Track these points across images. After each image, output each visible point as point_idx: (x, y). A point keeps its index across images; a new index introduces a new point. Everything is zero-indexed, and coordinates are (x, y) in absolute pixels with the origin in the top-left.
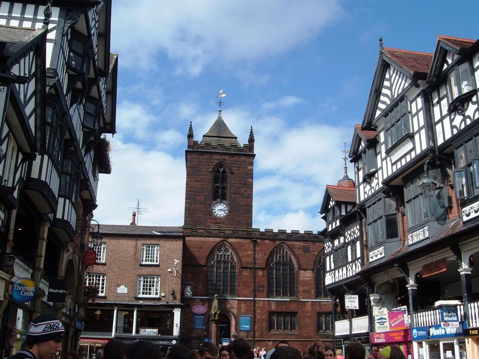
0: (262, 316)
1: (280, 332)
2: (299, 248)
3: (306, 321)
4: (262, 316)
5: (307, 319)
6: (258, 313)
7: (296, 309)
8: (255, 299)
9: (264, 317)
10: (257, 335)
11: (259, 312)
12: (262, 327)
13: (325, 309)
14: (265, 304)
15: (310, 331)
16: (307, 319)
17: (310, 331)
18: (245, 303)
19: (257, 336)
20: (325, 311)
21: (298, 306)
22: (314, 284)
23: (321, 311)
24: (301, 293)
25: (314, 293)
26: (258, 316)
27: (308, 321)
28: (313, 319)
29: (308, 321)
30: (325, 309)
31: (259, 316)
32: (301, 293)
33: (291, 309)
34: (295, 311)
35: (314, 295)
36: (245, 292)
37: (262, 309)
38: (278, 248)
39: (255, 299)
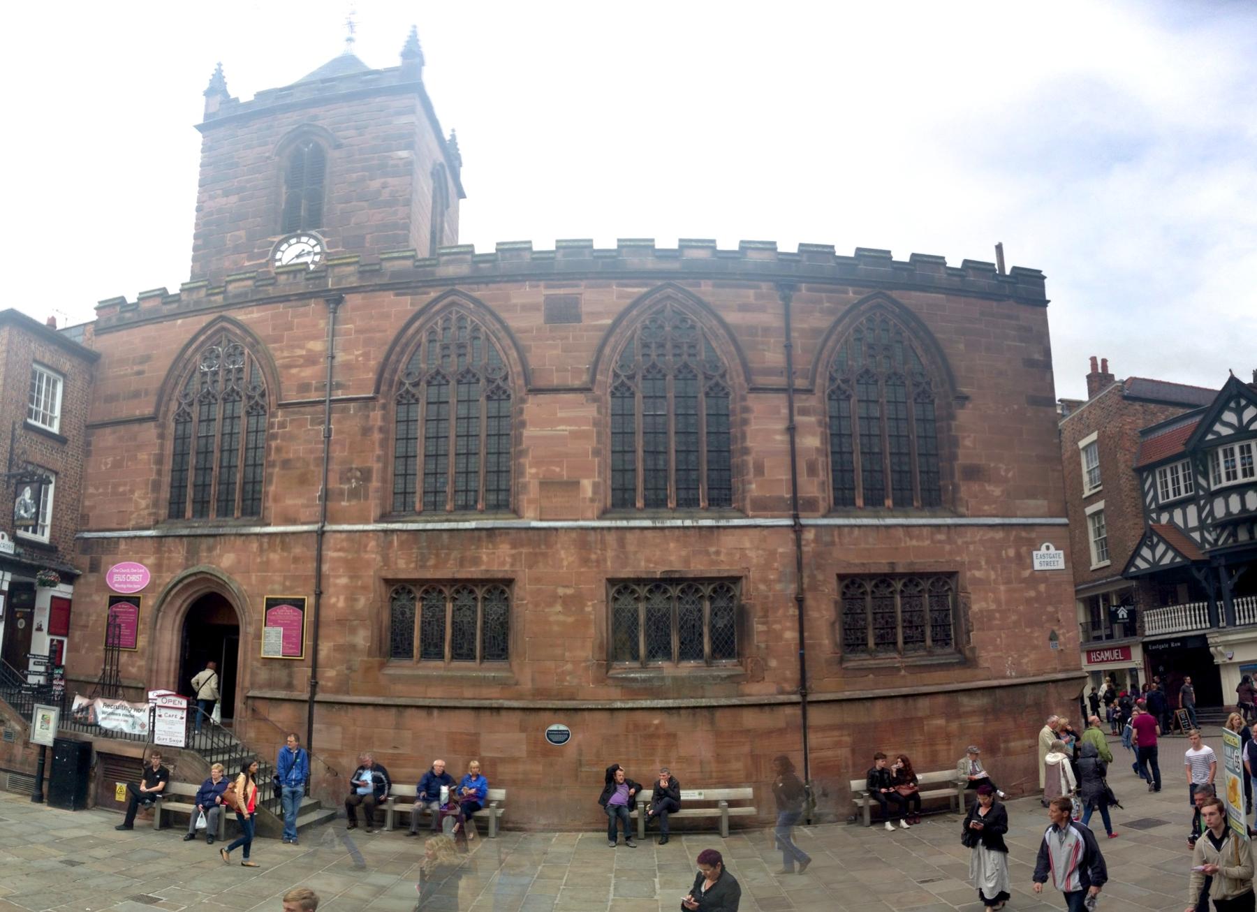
0: (351, 599)
1: (434, 668)
2: (534, 308)
3: (552, 619)
4: (356, 600)
5: (558, 608)
6: (335, 585)
7: (507, 567)
8: (328, 528)
9: (362, 602)
10: (329, 679)
11: (343, 581)
12: (353, 648)
13: (643, 564)
14: (368, 549)
15: (569, 667)
16: (558, 608)
17: (569, 667)
18: (285, 547)
19: (330, 684)
20: (647, 572)
21: (513, 552)
22: (596, 453)
23: (626, 573)
24: (533, 490)
25: (595, 492)
26: (338, 601)
27: (561, 618)
28: (589, 609)
29: (561, 618)
30: (643, 564)
31: (342, 598)
32: (533, 490)
33: (483, 568)
34: (500, 576)
35: (592, 500)
36: (292, 502)
37: (353, 568)
38: (438, 313)
39: (328, 528)
